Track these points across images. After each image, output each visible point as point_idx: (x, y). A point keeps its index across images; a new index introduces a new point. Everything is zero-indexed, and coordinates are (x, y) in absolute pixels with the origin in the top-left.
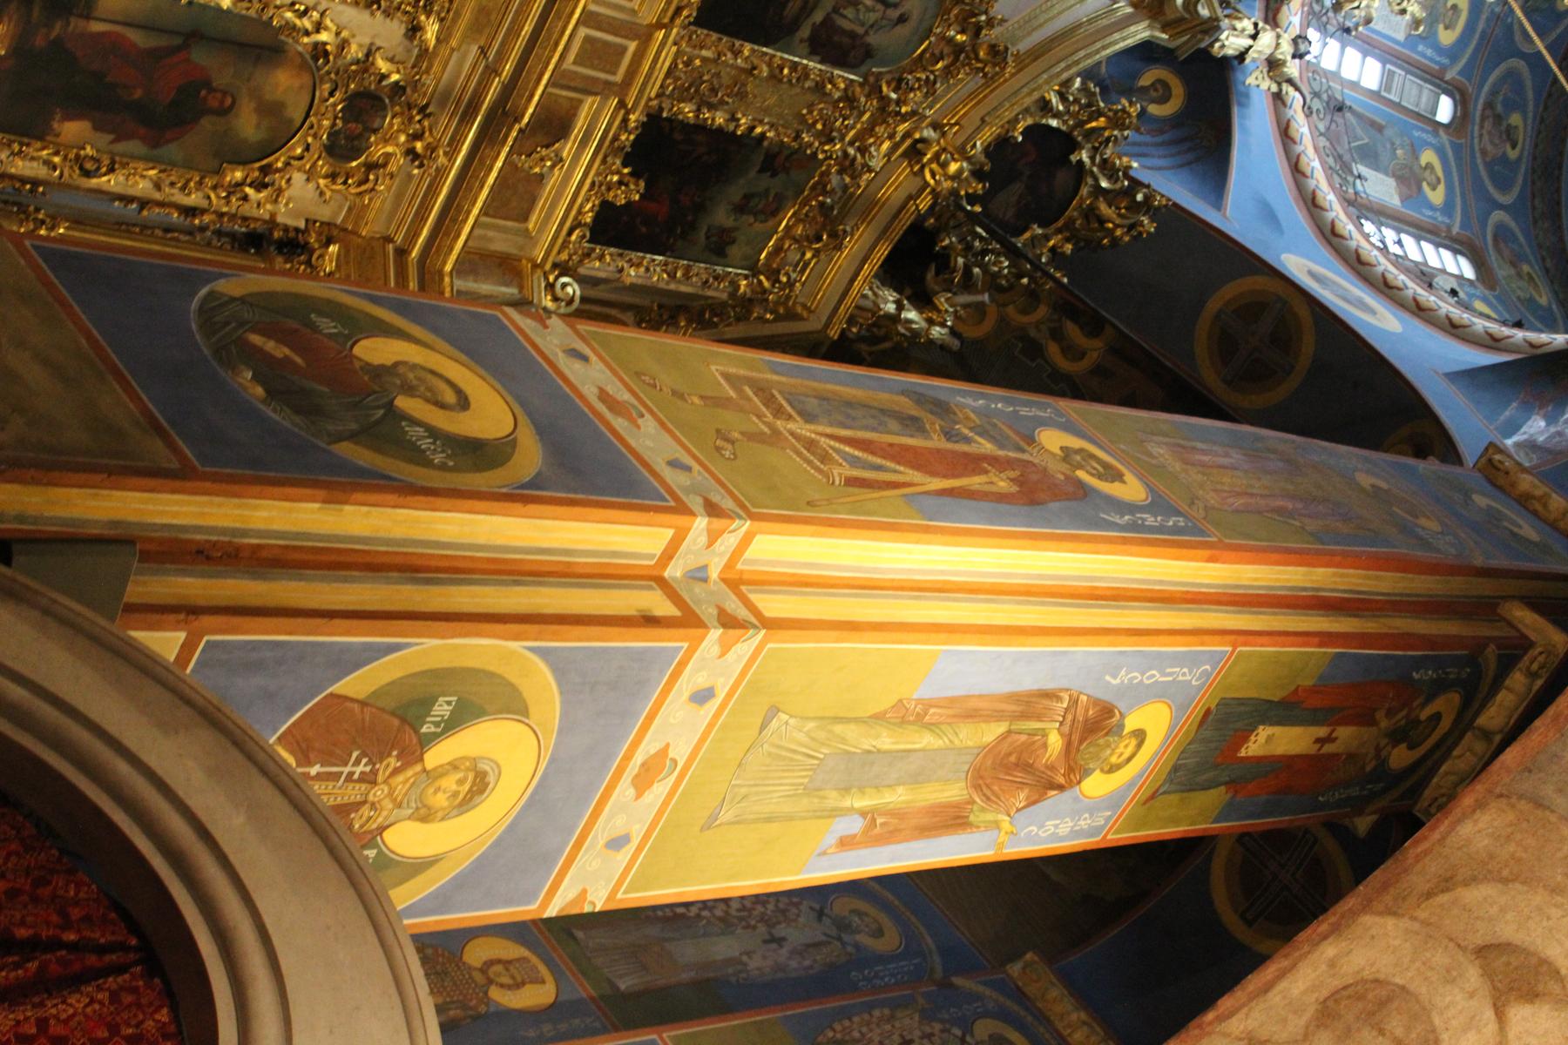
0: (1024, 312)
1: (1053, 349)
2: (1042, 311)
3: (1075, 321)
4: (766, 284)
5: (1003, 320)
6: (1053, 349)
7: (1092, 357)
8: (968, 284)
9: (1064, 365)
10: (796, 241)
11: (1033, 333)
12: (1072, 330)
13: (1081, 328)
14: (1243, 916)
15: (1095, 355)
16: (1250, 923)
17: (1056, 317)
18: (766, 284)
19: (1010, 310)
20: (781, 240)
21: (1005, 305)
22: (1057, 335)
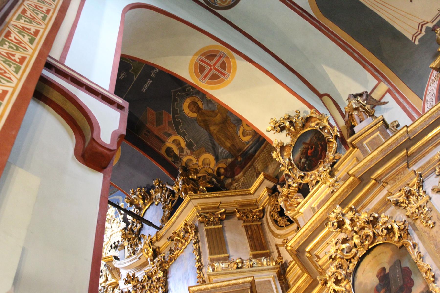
0: (191, 160)
1: (183, 145)
2: (185, 159)
3: (175, 154)
5: (198, 159)
6: (183, 145)
7: (170, 140)
9: (180, 138)
11: (189, 152)
12: (176, 151)
13: (173, 151)
15: (169, 141)
17: (181, 156)
19: (195, 162)
21: (196, 164)
22: (181, 150)
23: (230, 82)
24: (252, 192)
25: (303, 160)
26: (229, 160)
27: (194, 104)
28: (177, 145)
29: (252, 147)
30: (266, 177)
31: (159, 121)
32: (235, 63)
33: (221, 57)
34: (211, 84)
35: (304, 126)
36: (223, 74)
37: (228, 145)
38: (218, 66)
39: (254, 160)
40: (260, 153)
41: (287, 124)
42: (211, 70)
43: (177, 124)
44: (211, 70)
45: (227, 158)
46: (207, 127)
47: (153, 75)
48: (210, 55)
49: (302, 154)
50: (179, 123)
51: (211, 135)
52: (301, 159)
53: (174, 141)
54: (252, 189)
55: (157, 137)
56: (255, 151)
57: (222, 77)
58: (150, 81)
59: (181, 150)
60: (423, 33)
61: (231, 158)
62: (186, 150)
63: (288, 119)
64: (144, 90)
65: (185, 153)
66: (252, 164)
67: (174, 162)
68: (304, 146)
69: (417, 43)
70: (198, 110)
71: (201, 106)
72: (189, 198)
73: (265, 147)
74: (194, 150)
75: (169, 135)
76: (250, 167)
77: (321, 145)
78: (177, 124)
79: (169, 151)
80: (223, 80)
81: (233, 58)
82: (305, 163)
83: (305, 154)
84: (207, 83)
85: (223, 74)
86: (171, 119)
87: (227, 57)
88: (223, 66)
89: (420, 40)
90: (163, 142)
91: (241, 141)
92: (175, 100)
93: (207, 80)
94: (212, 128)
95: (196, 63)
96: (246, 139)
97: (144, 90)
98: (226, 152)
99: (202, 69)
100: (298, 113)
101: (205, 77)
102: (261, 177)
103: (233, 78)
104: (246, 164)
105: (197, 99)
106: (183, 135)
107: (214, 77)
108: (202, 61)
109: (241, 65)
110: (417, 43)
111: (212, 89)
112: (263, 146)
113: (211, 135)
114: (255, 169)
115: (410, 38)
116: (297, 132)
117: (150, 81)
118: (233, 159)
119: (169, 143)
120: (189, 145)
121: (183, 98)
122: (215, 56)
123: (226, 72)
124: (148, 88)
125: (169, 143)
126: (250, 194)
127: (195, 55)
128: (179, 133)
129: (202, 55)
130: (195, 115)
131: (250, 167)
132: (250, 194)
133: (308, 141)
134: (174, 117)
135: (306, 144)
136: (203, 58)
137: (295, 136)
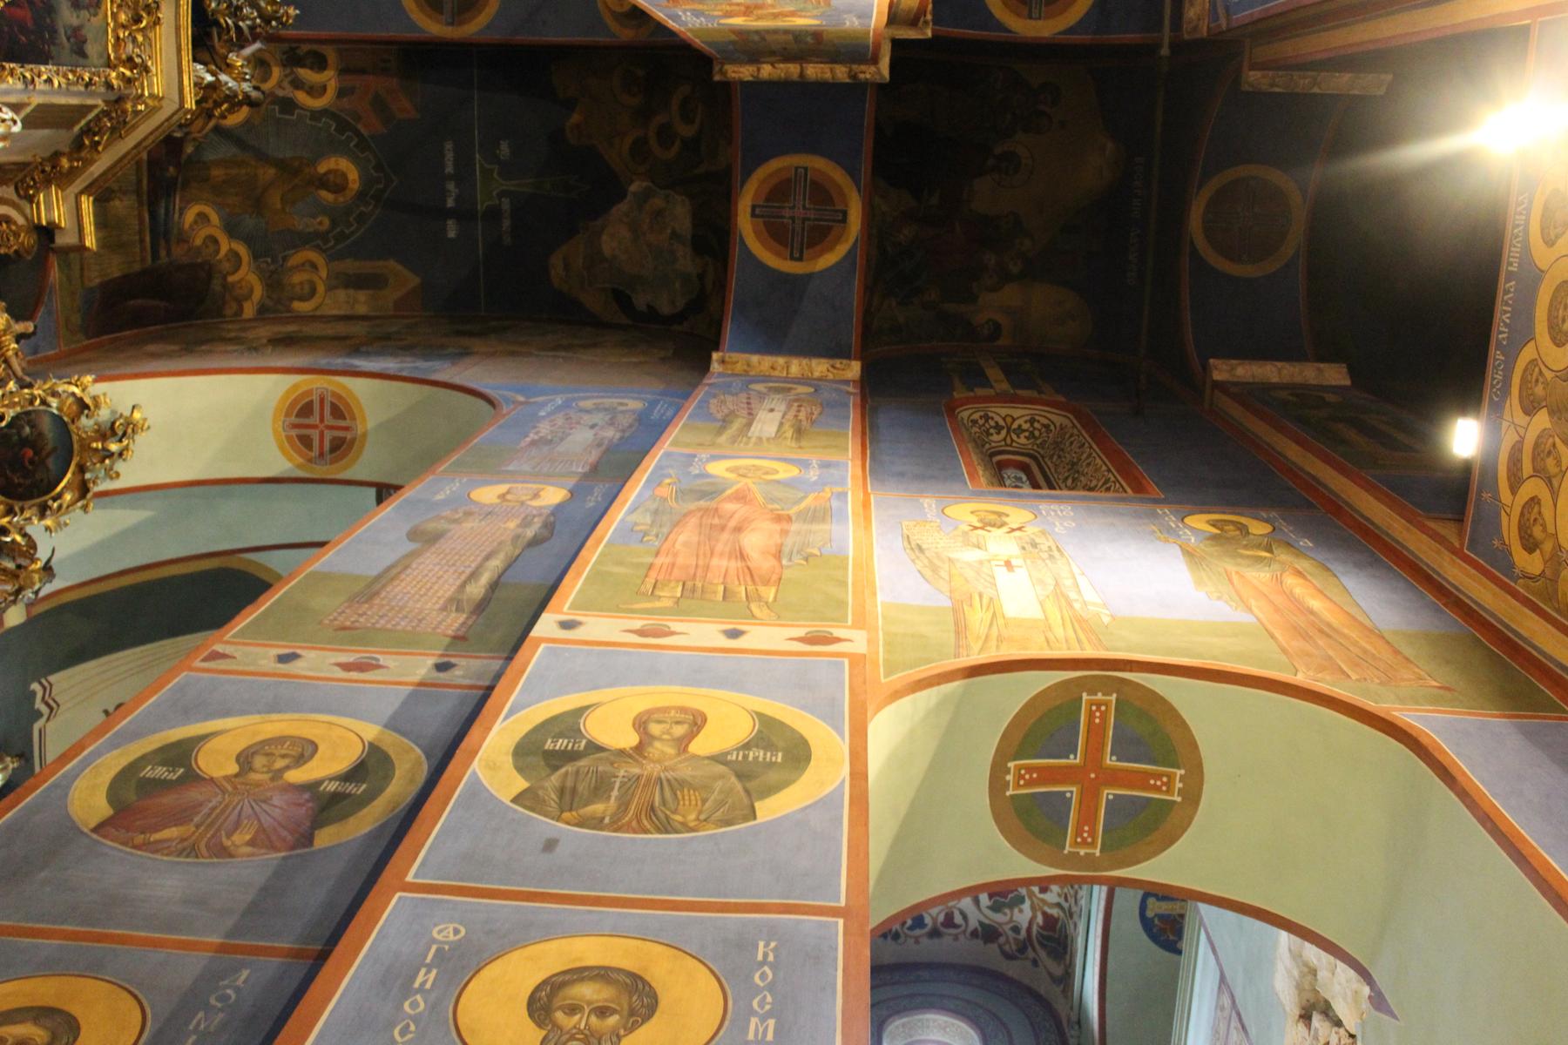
1: (301, 97)
2: (276, 72)
3: (303, 66)
4: (128, 73)
6: (301, 97)
8: (241, 42)
10: (124, 27)
11: (280, 93)
12: (305, 74)
13: (311, 68)
14: (792, 258)
16: (800, 259)
18: (128, 73)
20: (114, 30)
22: (297, 84)
23: (274, 422)
24: (84, 198)
25: (27, 430)
26: (189, 149)
27: (339, 187)
28: (311, 88)
29: (167, 213)
30: (81, 248)
31: (379, 105)
32: (290, 459)
33: (321, 454)
34: (292, 445)
35: (82, 469)
36: (295, 426)
37: (217, 173)
38: (315, 434)
39: (141, 203)
40: (141, 222)
41: (114, 447)
42: (322, 420)
43: (343, 126)
44: (322, 420)
45: (197, 149)
46: (281, 165)
47: (451, 186)
48: (341, 447)
49: (40, 434)
50: (338, 129)
51: (263, 157)
52: (33, 427)
53: (324, 88)
54: (87, 204)
55: (362, 71)
56: (153, 215)
57: (293, 419)
58: (449, 169)
59: (297, 84)
60: (39, 705)
61: (190, 156)
62: (288, 91)
63: (121, 454)
64: (449, 146)
65: (286, 84)
66: (138, 193)
67: (292, 49)
68: (49, 447)
69: (35, 686)
70: (323, 182)
71: (324, 193)
72: (187, 106)
73: (142, 241)
74: (273, 103)
75: (341, 93)
76: (139, 182)
77: (20, 485)
78: (343, 126)
79: (320, 63)
80: (287, 415)
81: (299, 466)
82: (19, 434)
83: (35, 442)
84: (309, 392)
85: (295, 426)
86: (359, 127)
87: (310, 461)
88: (306, 441)
89: (34, 693)
90: (344, 71)
91: (197, 200)
92: (379, 167)
93: (315, 398)
94: (272, 171)
95: (353, 418)
96: (190, 215)
97: (449, 146)
98: (210, 156)
99: (337, 412)
100: (112, 475)
101: (322, 401)
102: (90, 242)
103: (275, 431)
104: (151, 176)
105: (341, 199)
106: (316, 115)
107: (306, 410)
108: (347, 429)
109: (278, 463)
110: (35, 686)
111: (296, 386)
112: (148, 239)
113: (263, 157)
114: (125, 193)
115: (52, 678)
116: (85, 447)
117: (449, 169)
118: (184, 157)
119: (329, 78)
120: (288, 105)
121: (367, 181)
122: (333, 449)
123: (294, 433)
124: (443, 156)
125: (329, 78)
126: (82, 192)
127: (365, 435)
128: (324, 112)
129: (353, 440)
130: (322, 168)
131: (139, 182)
132: (82, 192)
133: (51, 463)
134: (358, 133)
135: (48, 455)
136: (349, 436)
137: (81, 439)
